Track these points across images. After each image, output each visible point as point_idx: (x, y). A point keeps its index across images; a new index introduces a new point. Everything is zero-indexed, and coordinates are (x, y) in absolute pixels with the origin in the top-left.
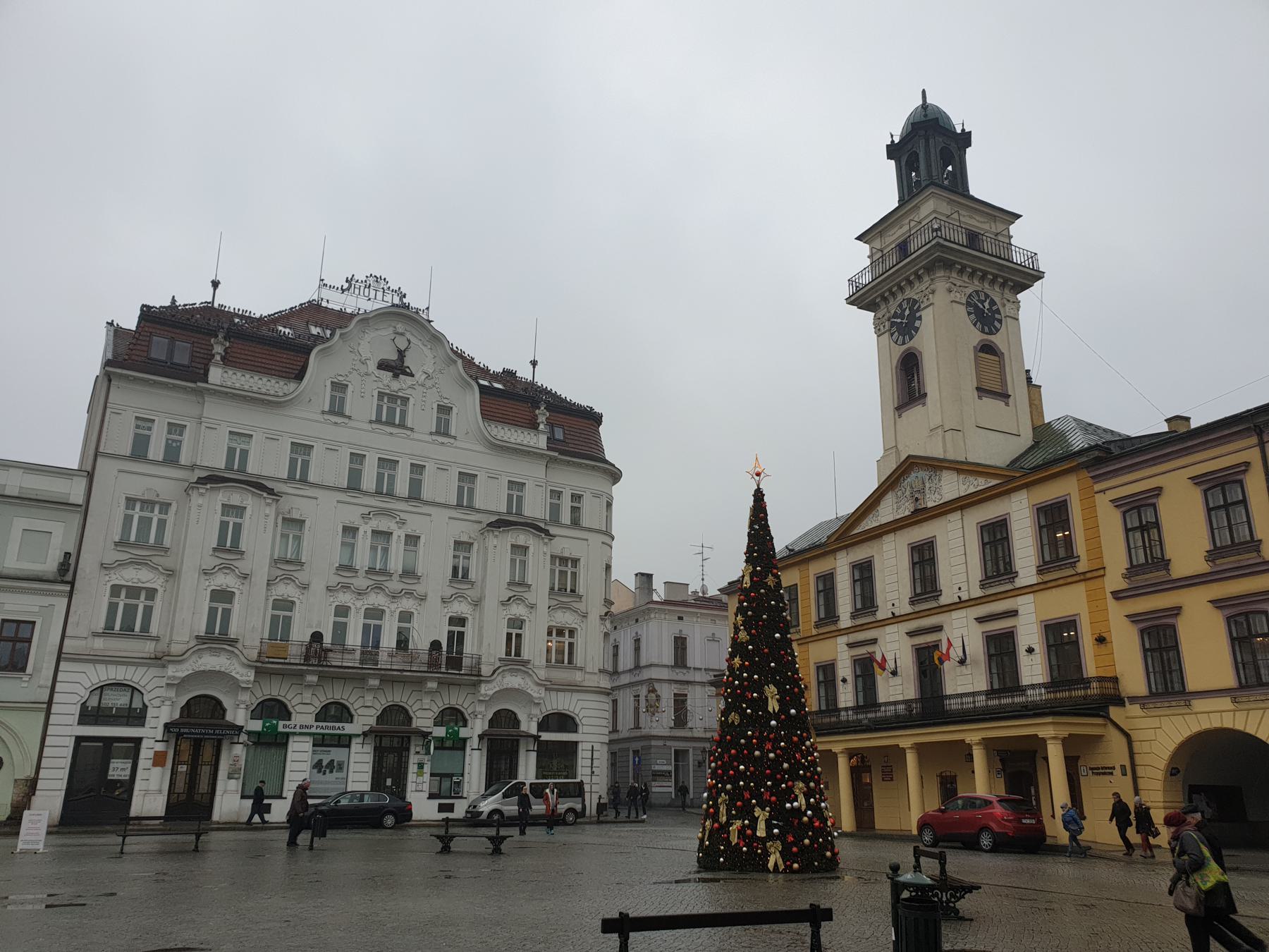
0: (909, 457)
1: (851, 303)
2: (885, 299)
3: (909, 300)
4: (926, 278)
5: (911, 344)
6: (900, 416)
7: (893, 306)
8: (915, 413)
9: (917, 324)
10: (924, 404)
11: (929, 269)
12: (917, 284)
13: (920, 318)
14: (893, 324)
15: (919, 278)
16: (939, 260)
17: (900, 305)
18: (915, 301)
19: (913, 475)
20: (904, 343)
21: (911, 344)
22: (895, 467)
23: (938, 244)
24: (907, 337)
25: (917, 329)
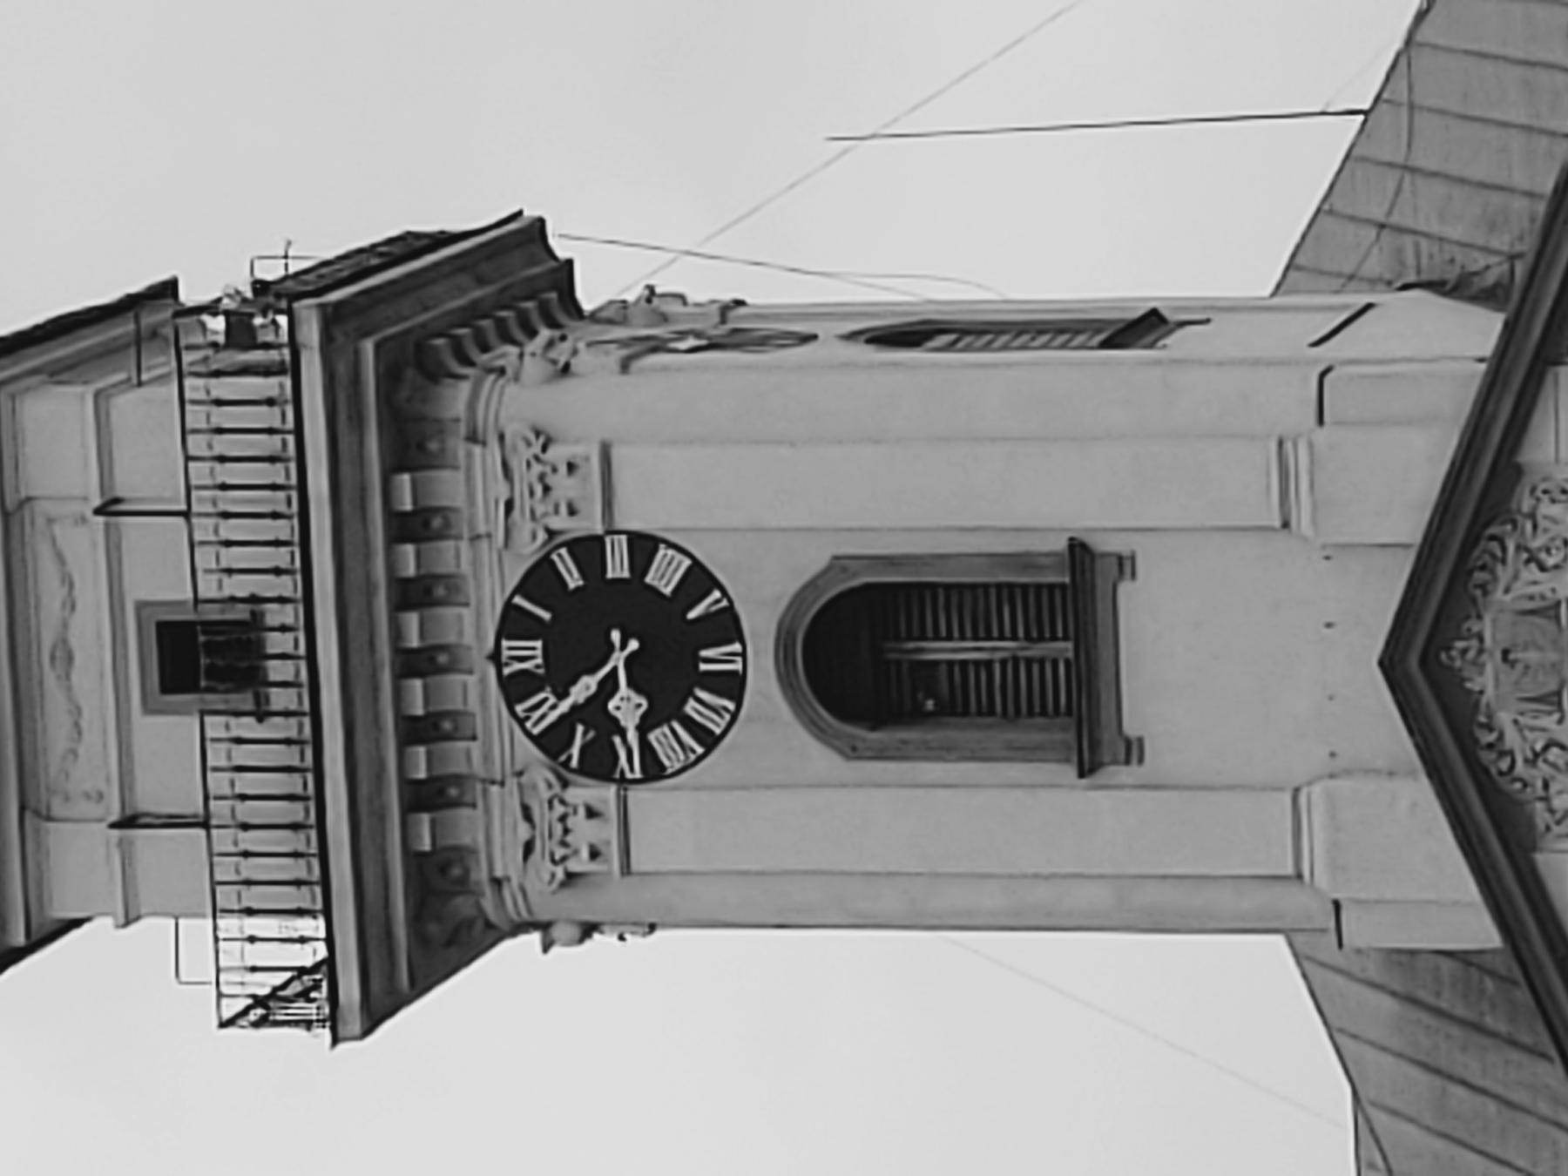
0: (1390, 664)
1: (373, 1018)
2: (430, 796)
3: (513, 623)
4: (448, 487)
5: (760, 627)
6: (1132, 751)
7: (499, 741)
8: (1160, 647)
9: (665, 575)
10: (1125, 565)
11: (412, 445)
12: (451, 556)
13: (644, 546)
14: (599, 765)
15: (414, 527)
16: (390, 377)
17: (516, 688)
18: (540, 579)
19: (1487, 681)
20: (732, 685)
21: (760, 627)
22: (1421, 791)
23: (332, 318)
24: (713, 658)
25: (699, 579)
